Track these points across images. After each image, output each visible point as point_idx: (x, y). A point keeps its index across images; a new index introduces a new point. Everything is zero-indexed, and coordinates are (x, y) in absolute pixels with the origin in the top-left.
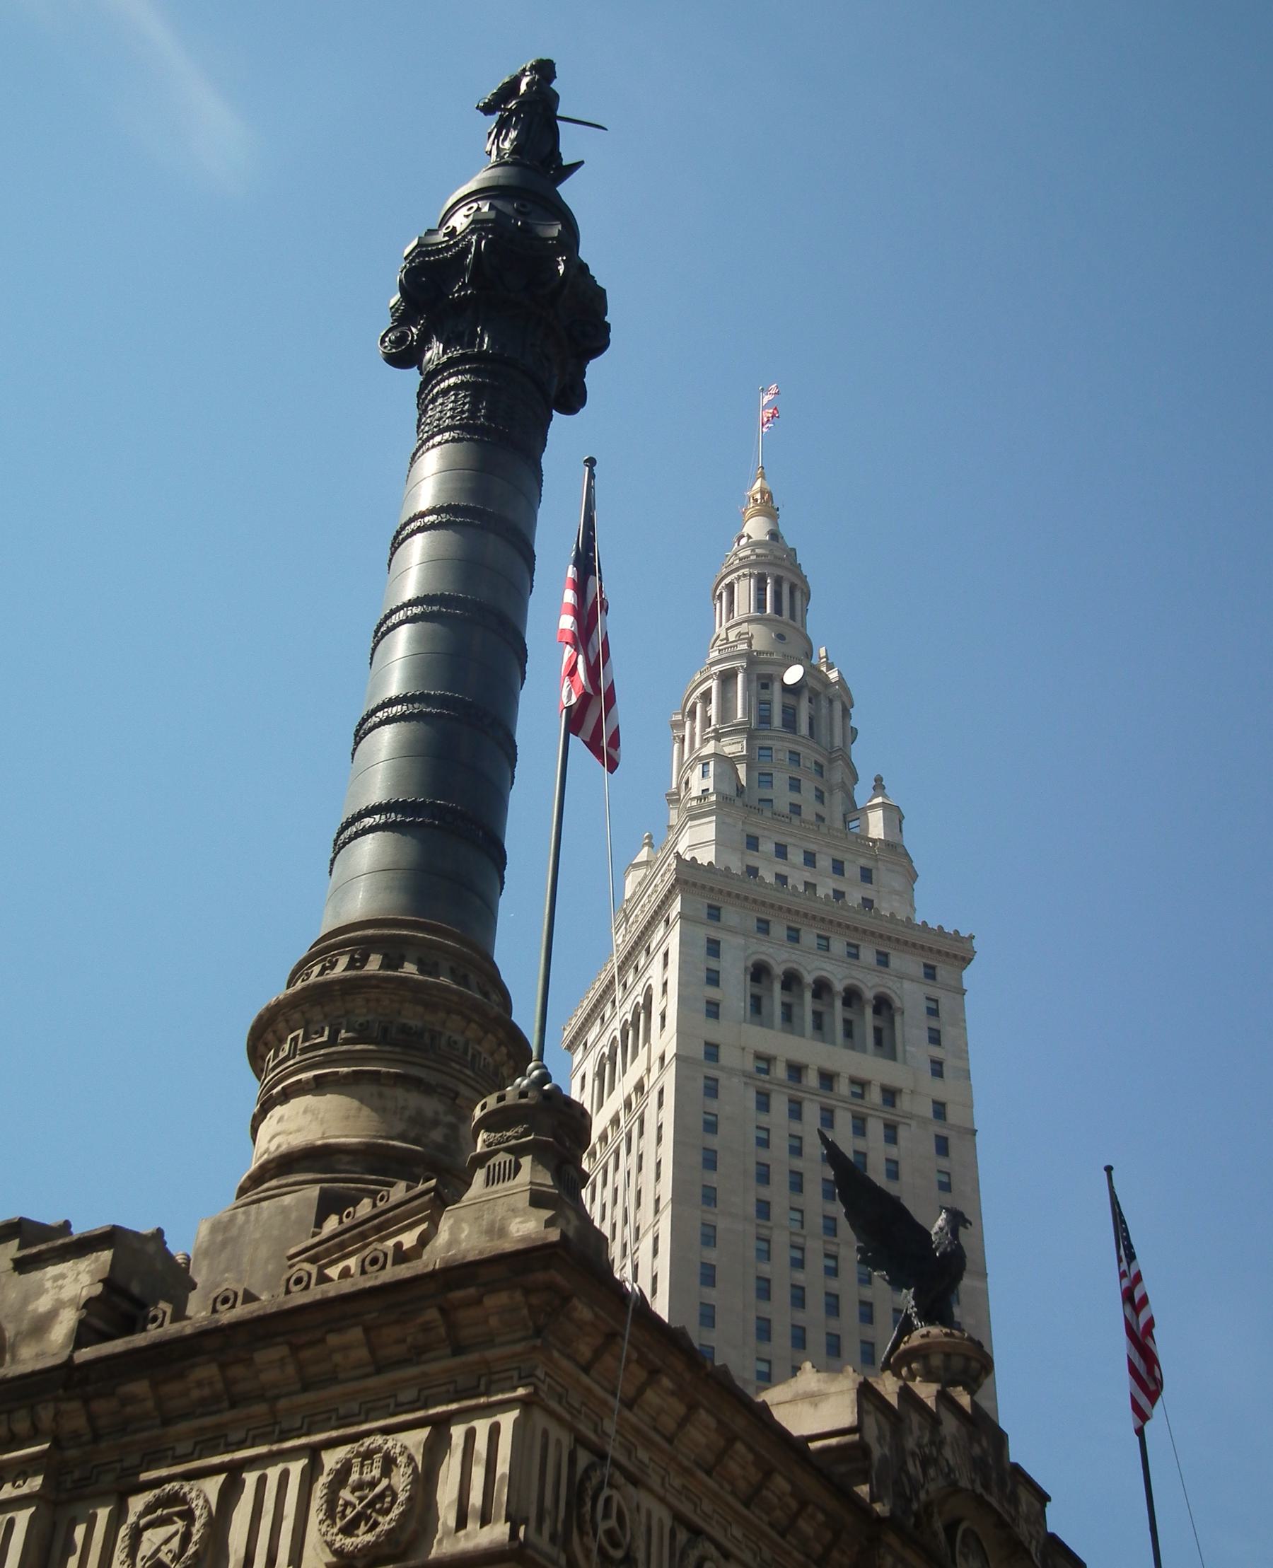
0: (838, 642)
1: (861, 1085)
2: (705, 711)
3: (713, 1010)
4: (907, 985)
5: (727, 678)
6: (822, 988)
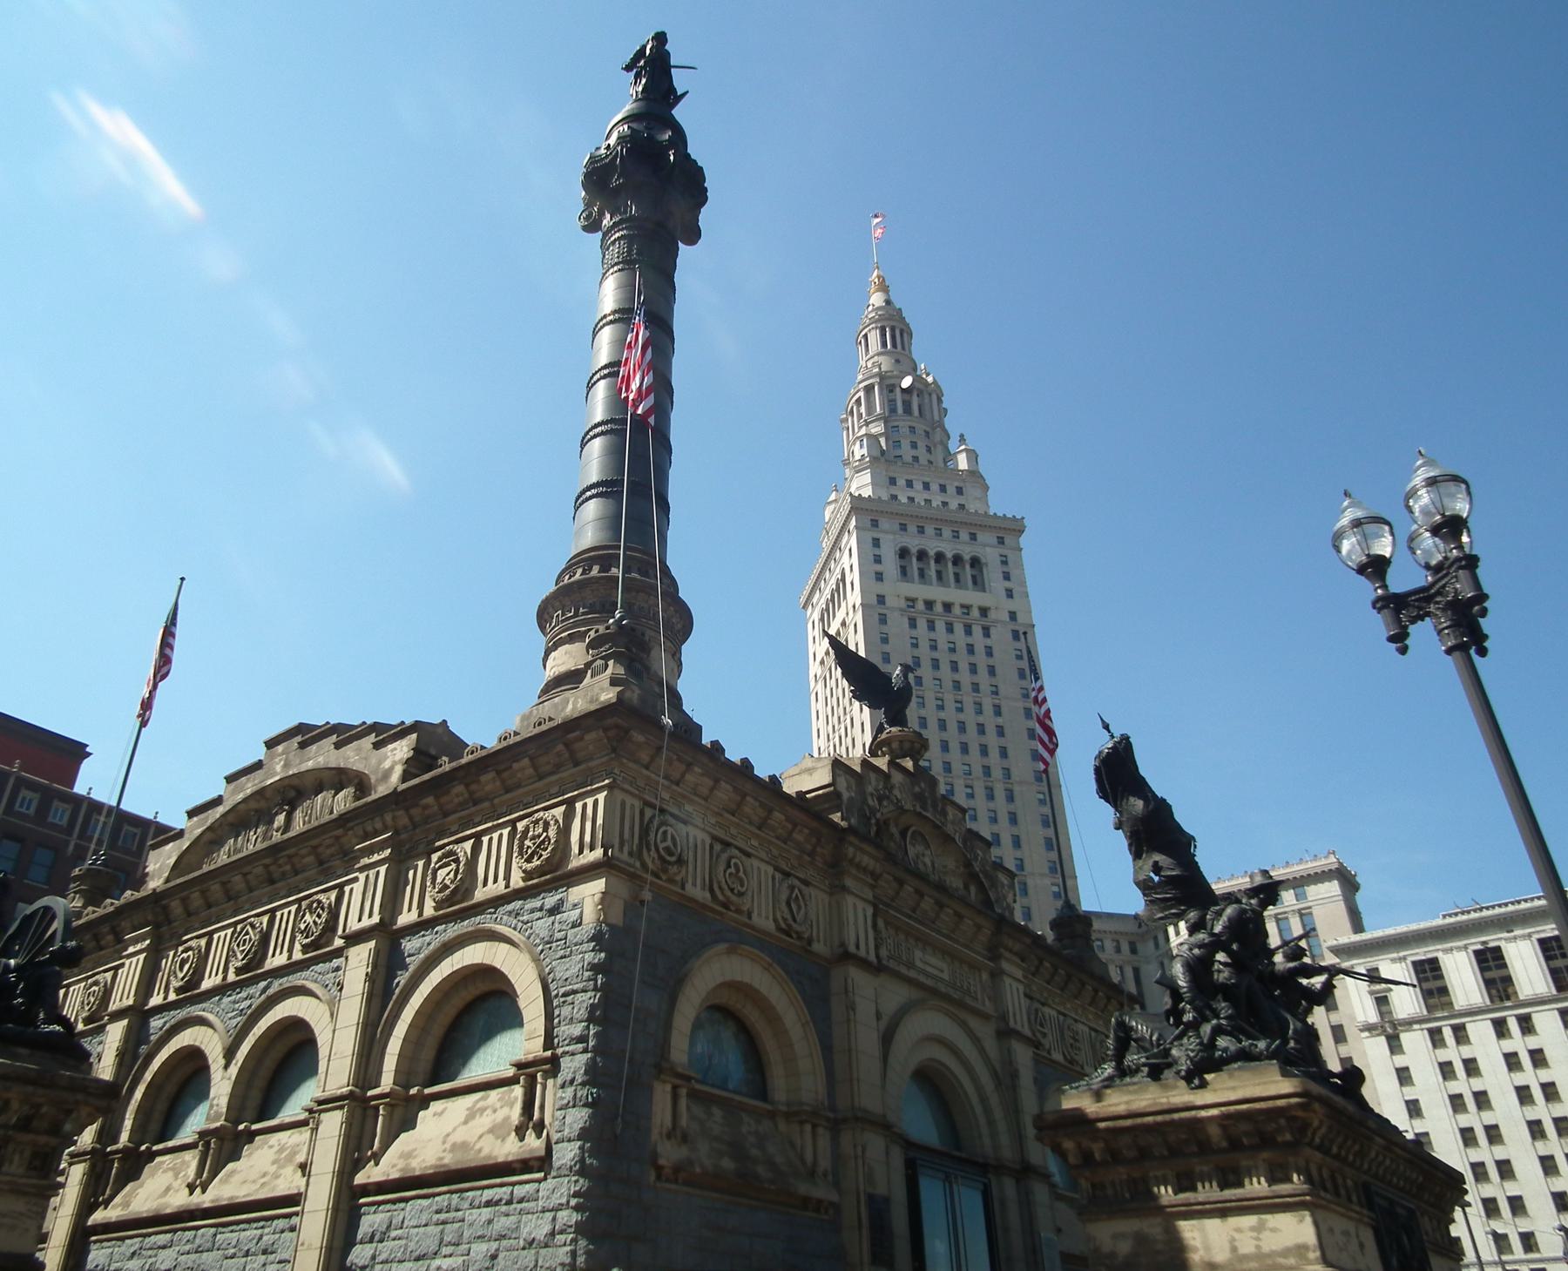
0: (931, 359)
1: (967, 608)
3: (879, 577)
4: (988, 549)
5: (869, 390)
6: (940, 557)
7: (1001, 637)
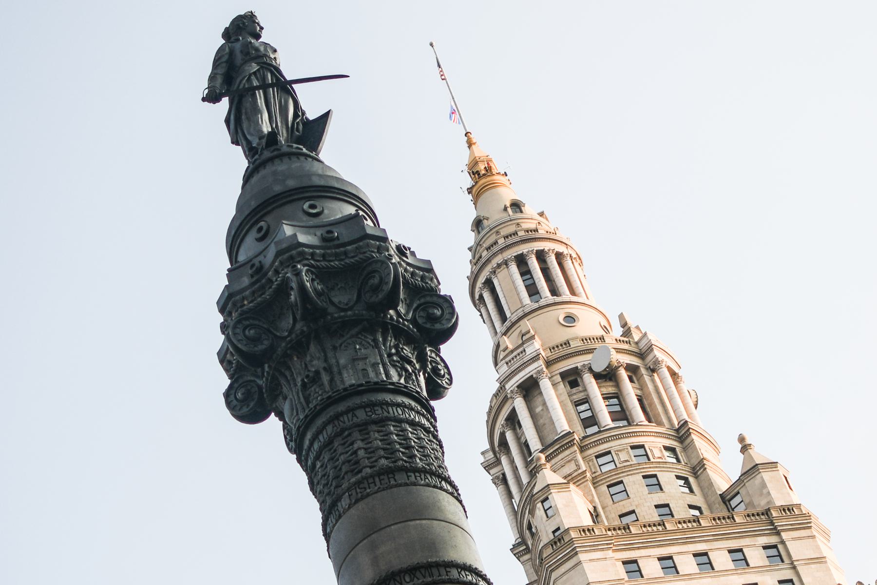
2: (518, 438)
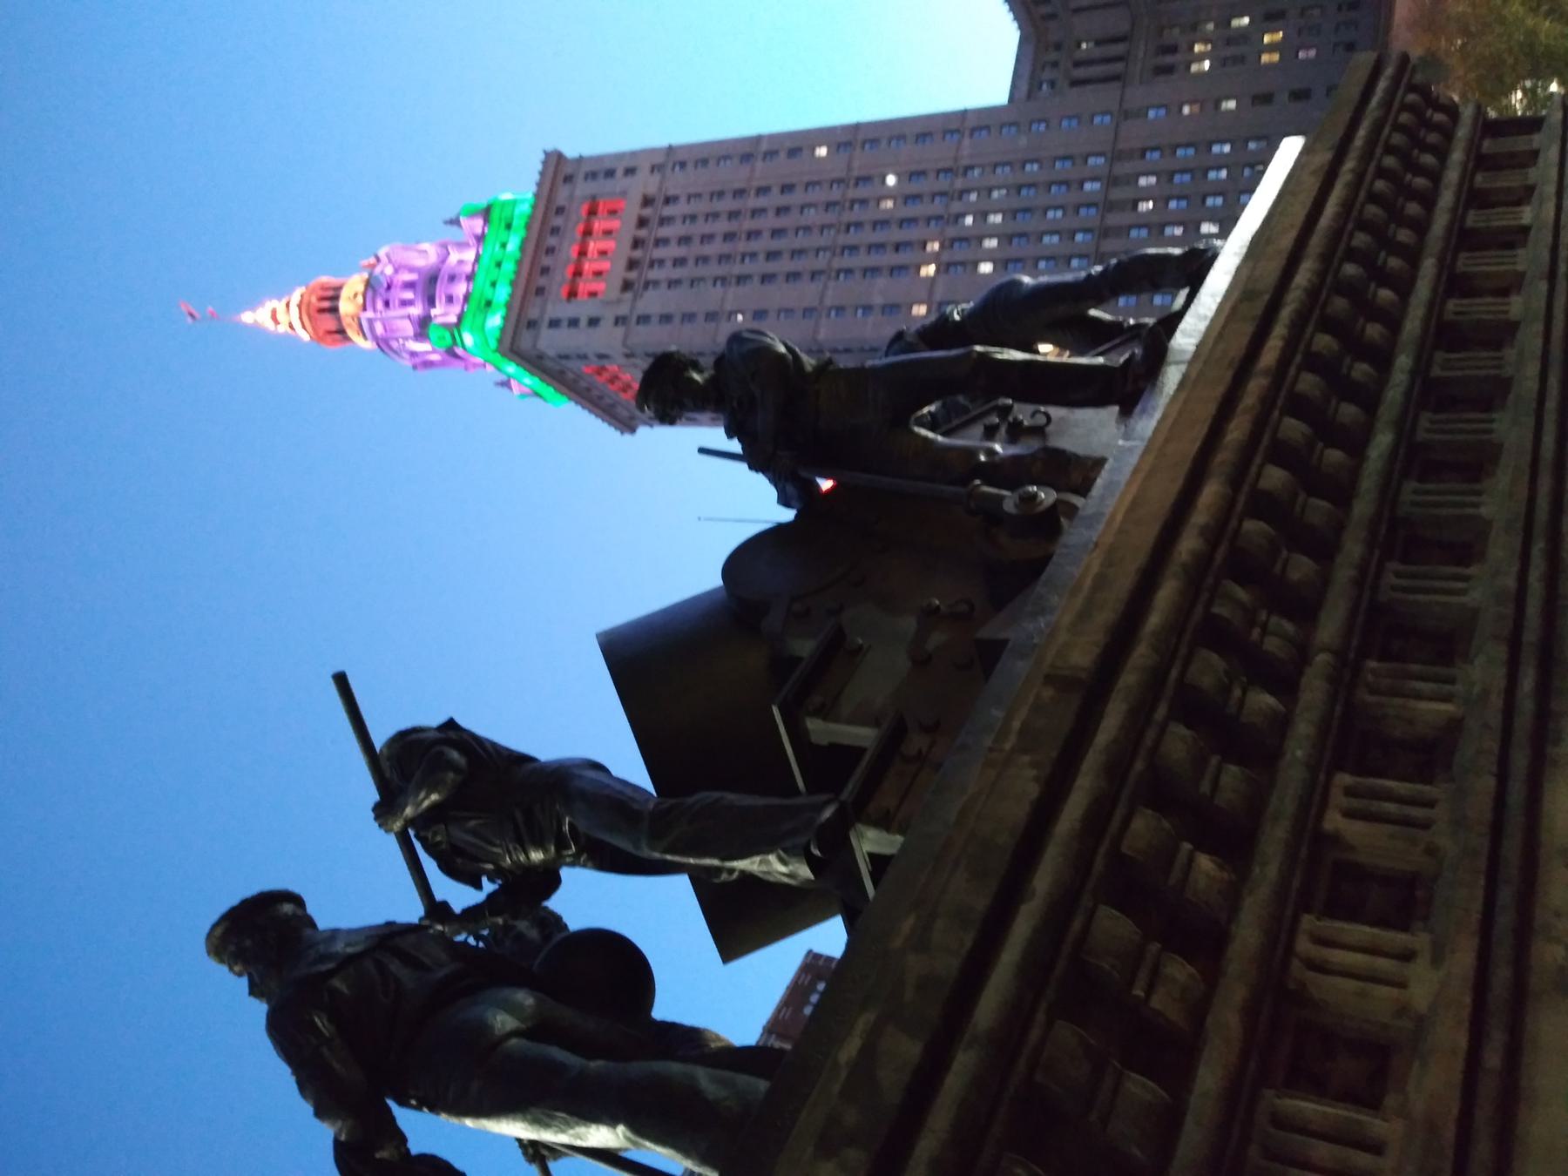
4: (578, 192)
7: (677, 182)
